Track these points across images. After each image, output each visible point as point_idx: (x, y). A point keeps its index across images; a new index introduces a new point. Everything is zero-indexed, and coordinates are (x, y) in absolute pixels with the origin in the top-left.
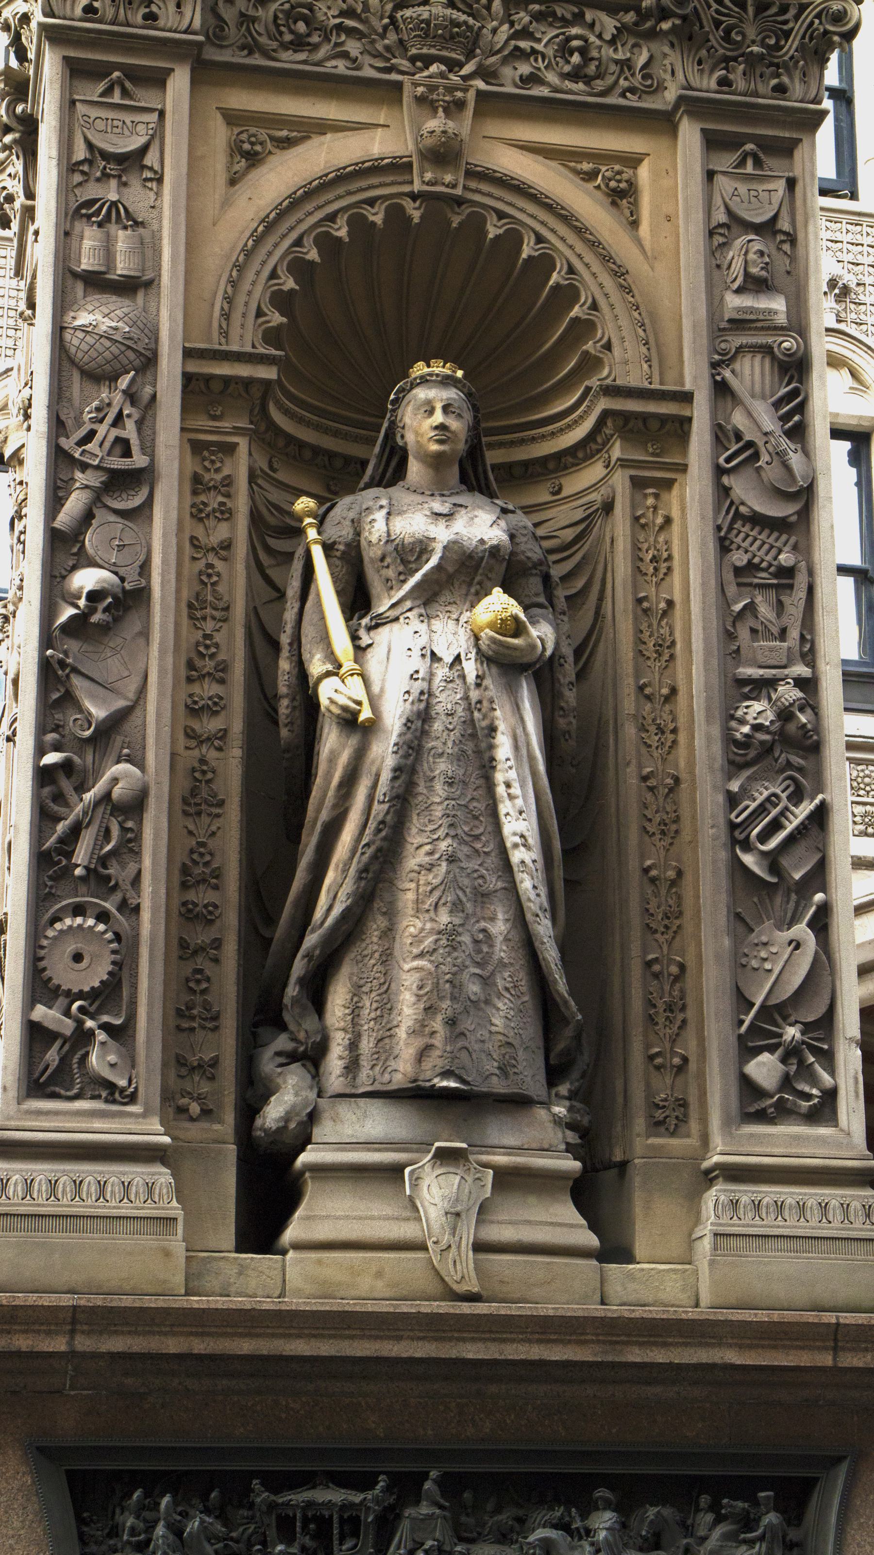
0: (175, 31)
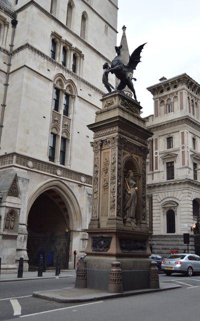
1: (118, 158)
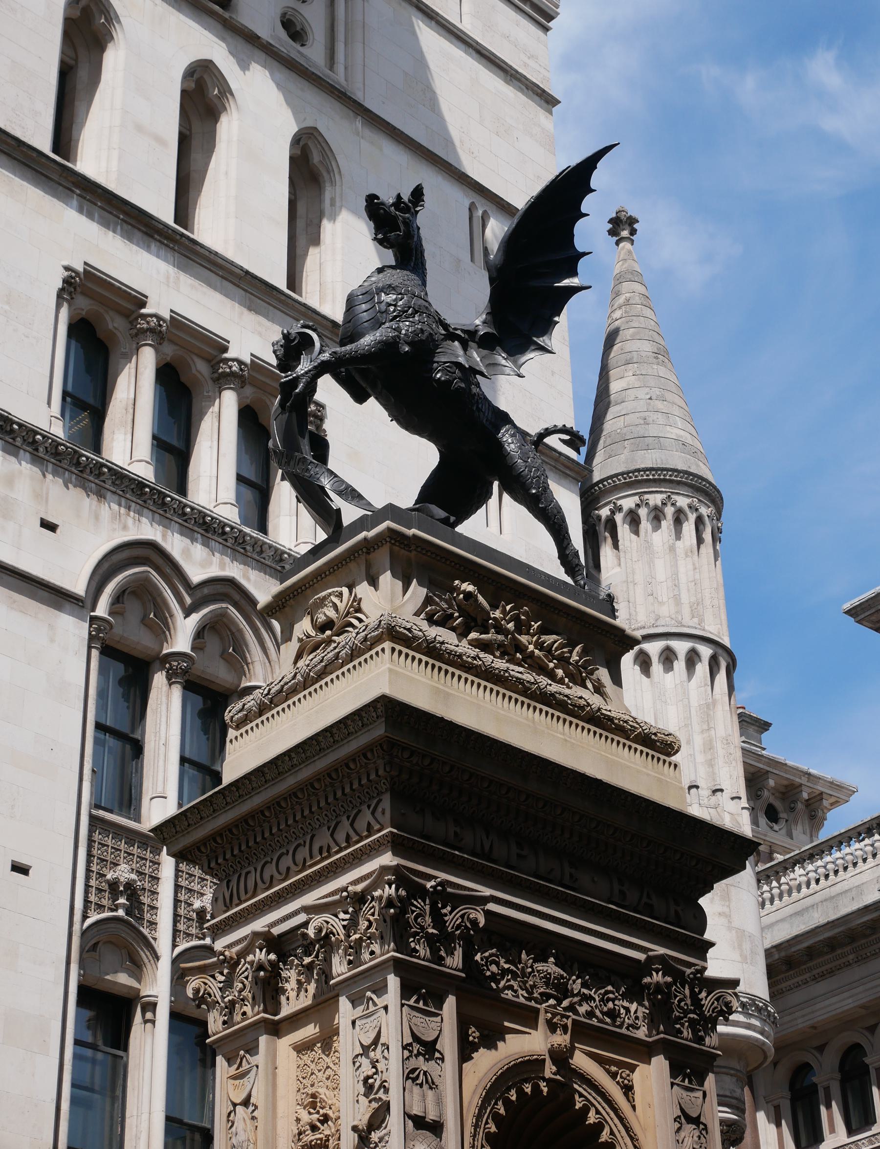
0: (451, 968)
1: (411, 1076)
